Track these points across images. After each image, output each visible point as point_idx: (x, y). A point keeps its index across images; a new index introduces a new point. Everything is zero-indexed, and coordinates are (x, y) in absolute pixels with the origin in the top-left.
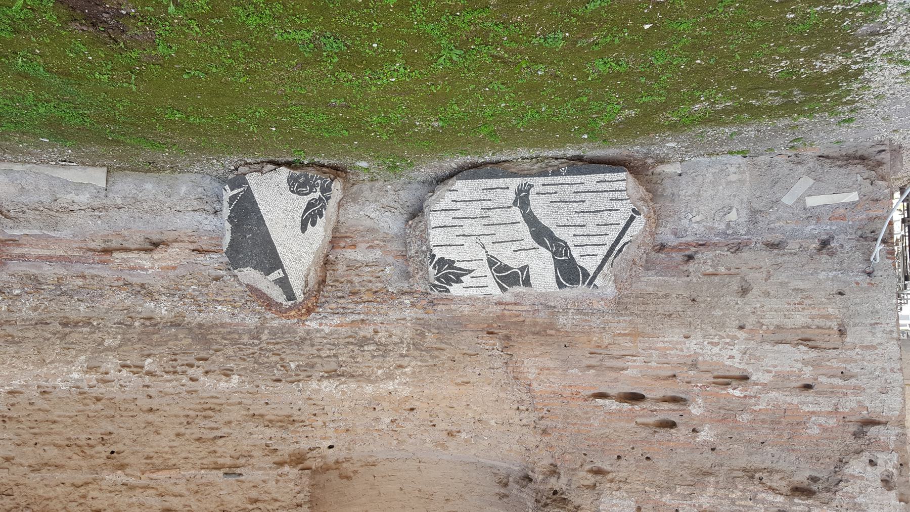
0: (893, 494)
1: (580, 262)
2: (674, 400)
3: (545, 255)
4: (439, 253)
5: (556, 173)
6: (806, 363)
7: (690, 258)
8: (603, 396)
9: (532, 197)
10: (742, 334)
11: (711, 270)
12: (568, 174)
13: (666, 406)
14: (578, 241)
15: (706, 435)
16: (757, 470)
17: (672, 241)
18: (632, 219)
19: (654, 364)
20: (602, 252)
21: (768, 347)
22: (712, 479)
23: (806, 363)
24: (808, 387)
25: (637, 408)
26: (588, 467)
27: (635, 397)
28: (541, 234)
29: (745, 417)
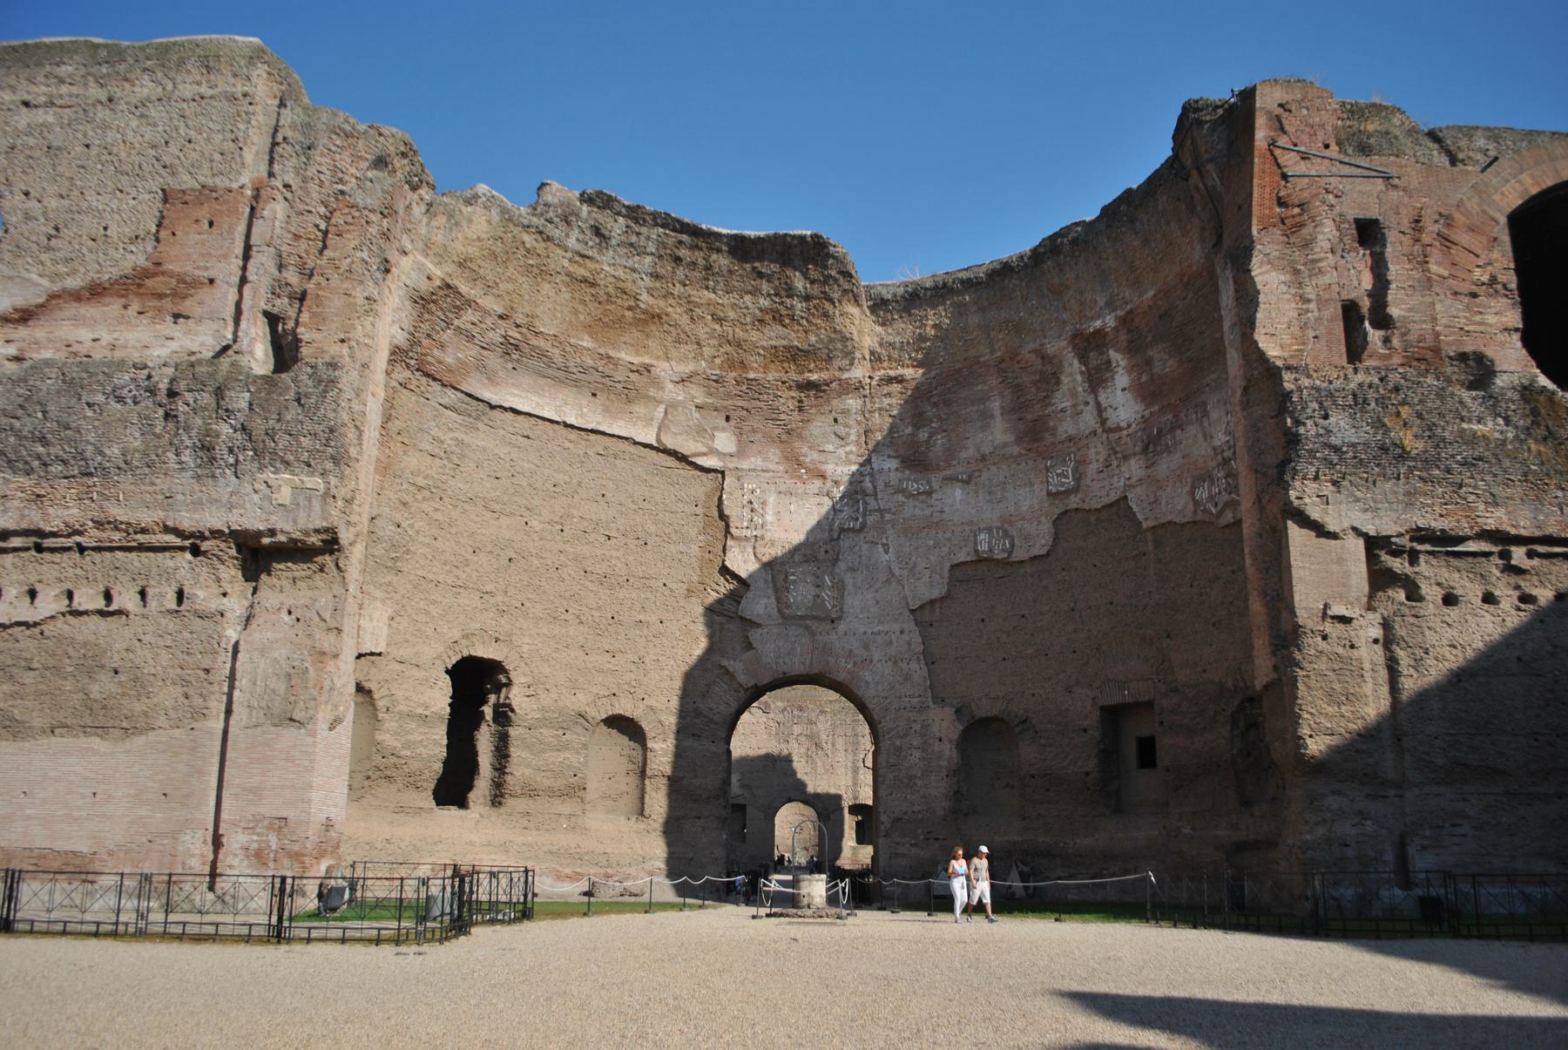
15: (920, 831)
24: (898, 844)
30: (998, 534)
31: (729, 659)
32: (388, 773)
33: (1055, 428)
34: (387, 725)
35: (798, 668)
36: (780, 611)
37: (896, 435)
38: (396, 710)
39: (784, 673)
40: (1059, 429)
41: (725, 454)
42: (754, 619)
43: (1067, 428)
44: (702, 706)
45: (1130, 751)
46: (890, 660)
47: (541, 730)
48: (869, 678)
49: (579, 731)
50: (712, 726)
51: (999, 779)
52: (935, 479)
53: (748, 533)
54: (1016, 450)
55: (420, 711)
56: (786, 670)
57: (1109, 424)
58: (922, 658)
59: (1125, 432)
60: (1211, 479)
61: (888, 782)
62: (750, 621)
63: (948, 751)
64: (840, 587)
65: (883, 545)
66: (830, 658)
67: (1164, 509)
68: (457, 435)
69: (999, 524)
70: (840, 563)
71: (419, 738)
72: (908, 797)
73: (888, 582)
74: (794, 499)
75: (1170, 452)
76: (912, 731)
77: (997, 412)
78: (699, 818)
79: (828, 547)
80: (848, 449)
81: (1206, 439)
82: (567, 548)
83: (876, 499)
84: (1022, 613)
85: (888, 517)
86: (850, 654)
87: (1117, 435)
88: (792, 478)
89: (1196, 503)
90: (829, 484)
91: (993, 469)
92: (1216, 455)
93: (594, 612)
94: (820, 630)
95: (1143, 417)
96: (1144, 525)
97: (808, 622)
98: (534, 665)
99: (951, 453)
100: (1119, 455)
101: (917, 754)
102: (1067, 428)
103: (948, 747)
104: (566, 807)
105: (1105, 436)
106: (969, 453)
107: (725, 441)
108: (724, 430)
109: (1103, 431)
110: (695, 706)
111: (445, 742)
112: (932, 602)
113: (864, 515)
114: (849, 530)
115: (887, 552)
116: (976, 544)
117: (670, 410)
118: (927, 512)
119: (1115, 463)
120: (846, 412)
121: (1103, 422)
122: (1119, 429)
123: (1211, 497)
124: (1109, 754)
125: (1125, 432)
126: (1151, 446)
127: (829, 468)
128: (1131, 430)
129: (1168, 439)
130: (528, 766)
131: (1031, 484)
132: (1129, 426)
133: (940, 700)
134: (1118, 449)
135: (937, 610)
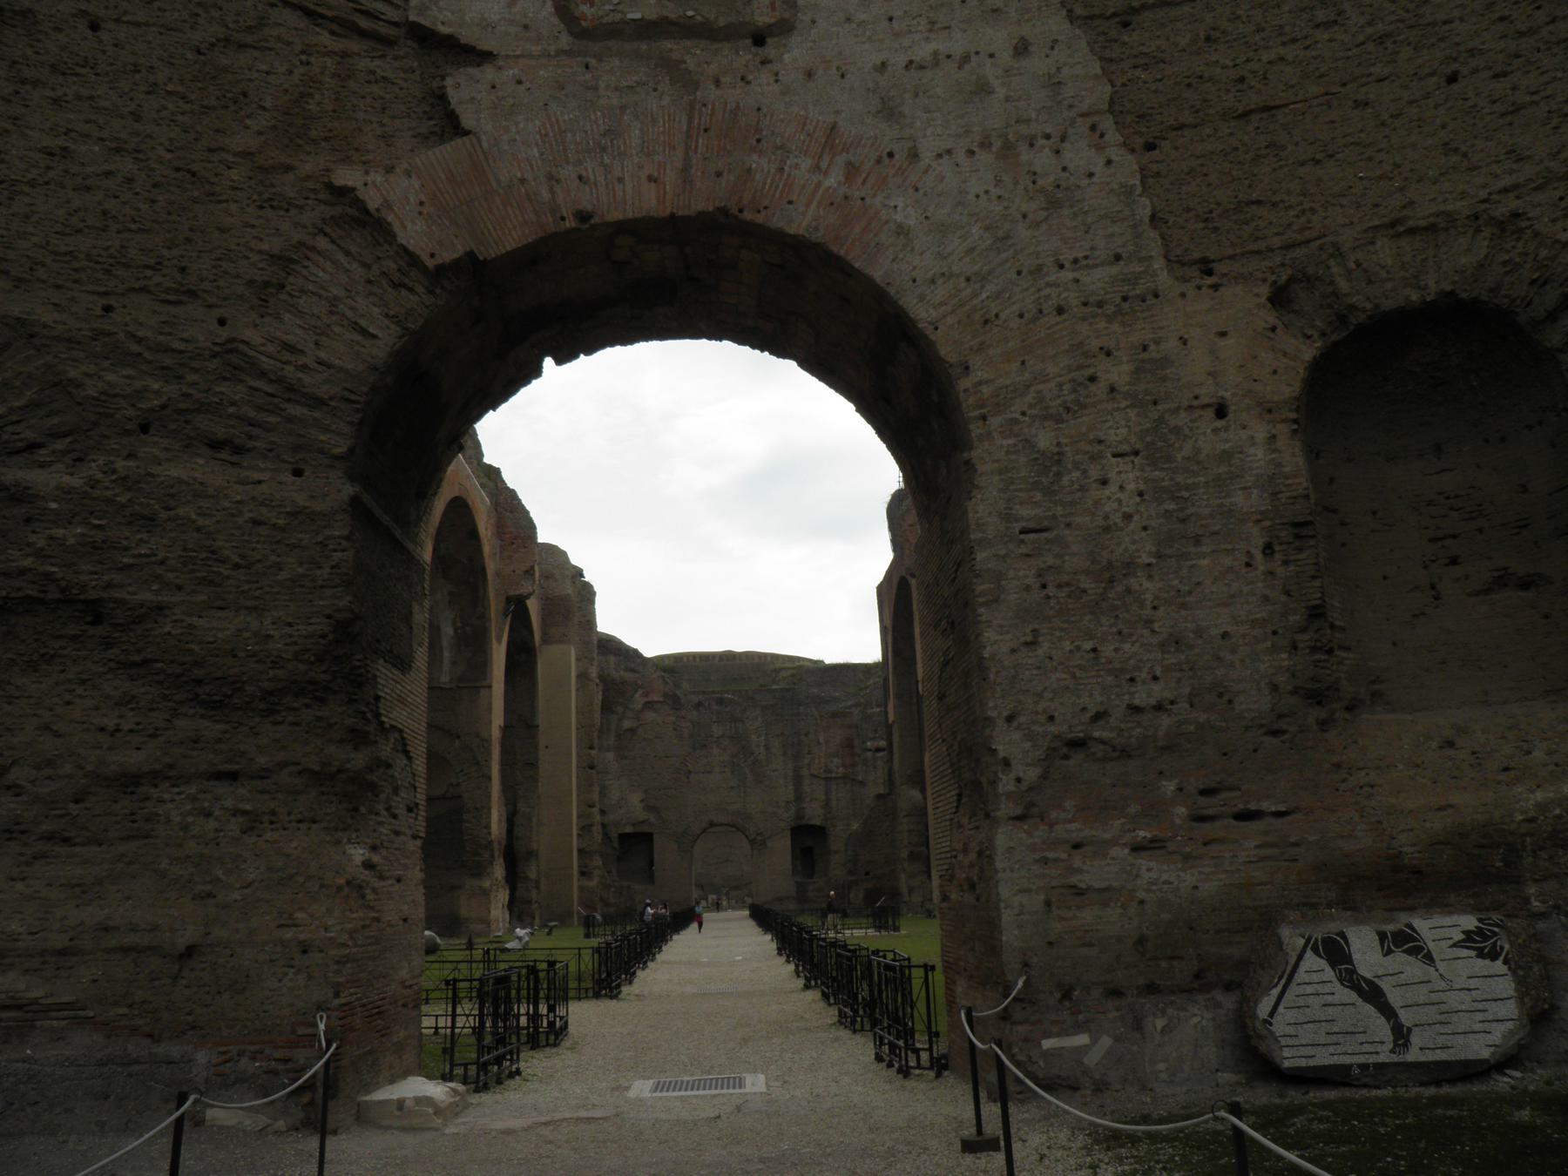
0: (1002, 754)
1: (1323, 963)
2: (1202, 819)
3: (1364, 971)
4: (1499, 966)
5: (1364, 1067)
6: (1079, 871)
7: (1197, 976)
8: (1279, 814)
10: (1141, 895)
11: (1175, 963)
12: (1351, 1066)
13: (1211, 812)
14: (1327, 988)
15: (1169, 787)
16: (1119, 758)
17: (1218, 995)
18: (1272, 1014)
19: (1227, 855)
20: (1301, 976)
21: (1115, 884)
22: (1160, 743)
23: (1079, 871)
24: (1077, 846)
25: (1241, 806)
26: (1286, 736)
28: (1372, 994)
29: (1134, 809)
39: (583, 217)
42: (467, 36)
44: (249, 334)
46: (985, 144)
50: (296, 410)
51: (1454, 561)
56: (588, 206)
58: (1107, 123)
66: (754, 161)
72: (1108, 650)
76: (1099, 389)
78: (233, 776)
97: (668, 44)
101: (1129, 476)
103: (1260, 431)
110: (223, 334)
133: (1194, 272)
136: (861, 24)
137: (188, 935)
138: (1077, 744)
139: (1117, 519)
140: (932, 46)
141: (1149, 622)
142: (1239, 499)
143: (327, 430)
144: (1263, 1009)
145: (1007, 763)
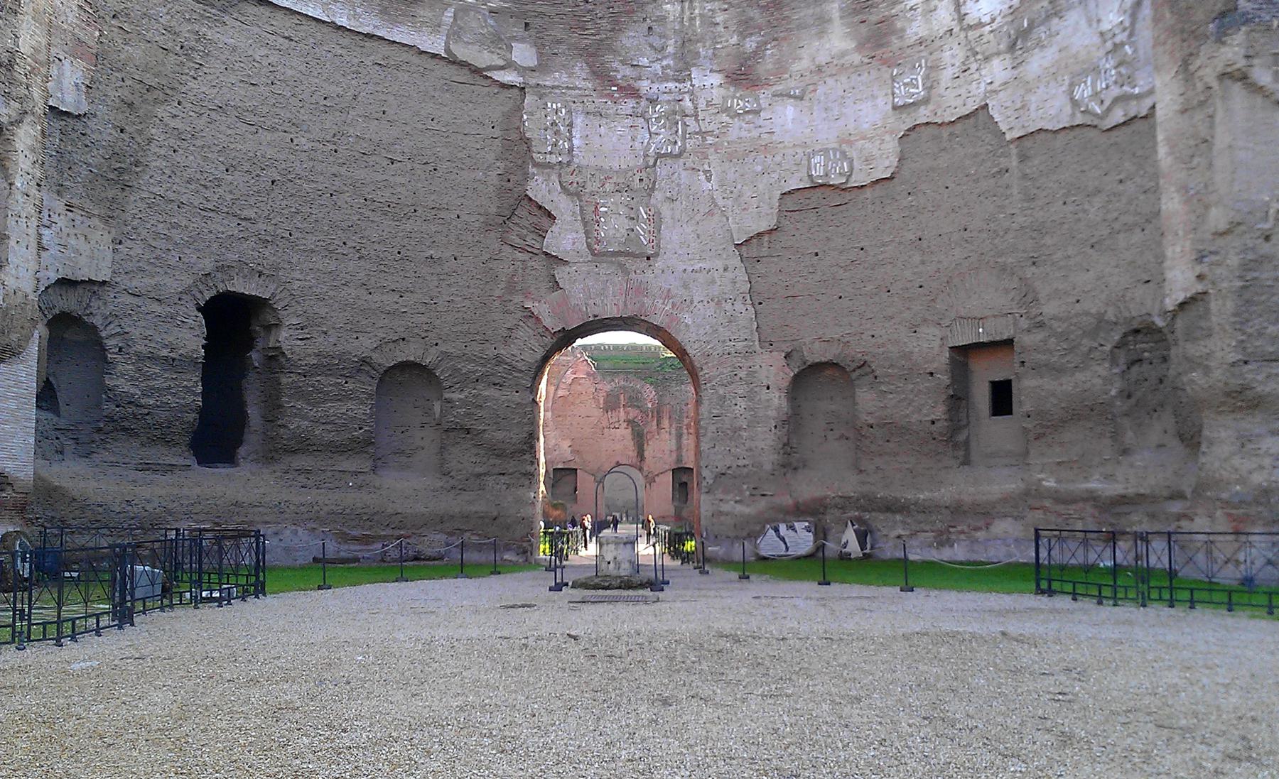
2: (753, 495)
4: (811, 534)
9: (784, 549)
15: (745, 487)
24: (721, 500)
27: (763, 495)
28: (783, 539)
30: (835, 155)
31: (534, 300)
32: (126, 424)
33: (903, 30)
34: (120, 368)
35: (610, 310)
36: (589, 246)
37: (719, 46)
38: (131, 351)
40: (908, 31)
41: (525, 69)
43: (916, 29)
45: (982, 397)
47: (319, 378)
48: (689, 321)
49: (362, 379)
50: (516, 375)
51: (832, 430)
52: (764, 96)
53: (553, 159)
54: (856, 58)
55: (164, 353)
57: (970, 20)
59: (988, 28)
60: (1096, 70)
61: (709, 434)
62: (556, 257)
63: (776, 401)
64: (656, 220)
65: (705, 172)
67: (1033, 115)
68: (197, 27)
69: (836, 145)
70: (656, 192)
71: (167, 384)
72: (732, 450)
73: (710, 213)
74: (604, 121)
75: (1043, 47)
76: (737, 378)
77: (836, 15)
78: (504, 474)
79: (643, 175)
80: (665, 63)
81: (1090, 25)
82: (343, 170)
83: (697, 121)
84: (861, 245)
85: (710, 140)
86: (668, 295)
87: (977, 33)
88: (602, 97)
89: (1075, 103)
90: (644, 103)
91: (830, 81)
92: (1105, 41)
93: (376, 246)
94: (634, 267)
95: (1010, 7)
96: (1008, 137)
97: (621, 259)
98: (307, 303)
99: (781, 69)
100: (979, 57)
101: (742, 403)
102: (916, 29)
104: (348, 464)
105: (962, 35)
106: (804, 64)
107: (524, 54)
108: (522, 40)
109: (961, 30)
110: (496, 352)
111: (200, 389)
112: (760, 235)
113: (684, 138)
114: (665, 155)
115: (709, 180)
116: (809, 168)
117: (460, 14)
118: (755, 133)
119: (974, 66)
120: (662, 19)
121: (962, 18)
122: (981, 25)
123: (1096, 94)
124: (958, 399)
125: (988, 28)
126: (1019, 42)
127: (644, 85)
128: (995, 26)
129: (1041, 32)
130: (304, 418)
131: (874, 97)
132: (993, 20)
133: (767, 344)
134: (978, 49)
135: (766, 244)
136: (680, 255)
137: (495, 514)
138: (723, 474)
139: (738, 415)
140: (701, 265)
141: (744, 444)
142: (769, 413)
143: (525, 380)
144: (758, 542)
145: (705, 478)
